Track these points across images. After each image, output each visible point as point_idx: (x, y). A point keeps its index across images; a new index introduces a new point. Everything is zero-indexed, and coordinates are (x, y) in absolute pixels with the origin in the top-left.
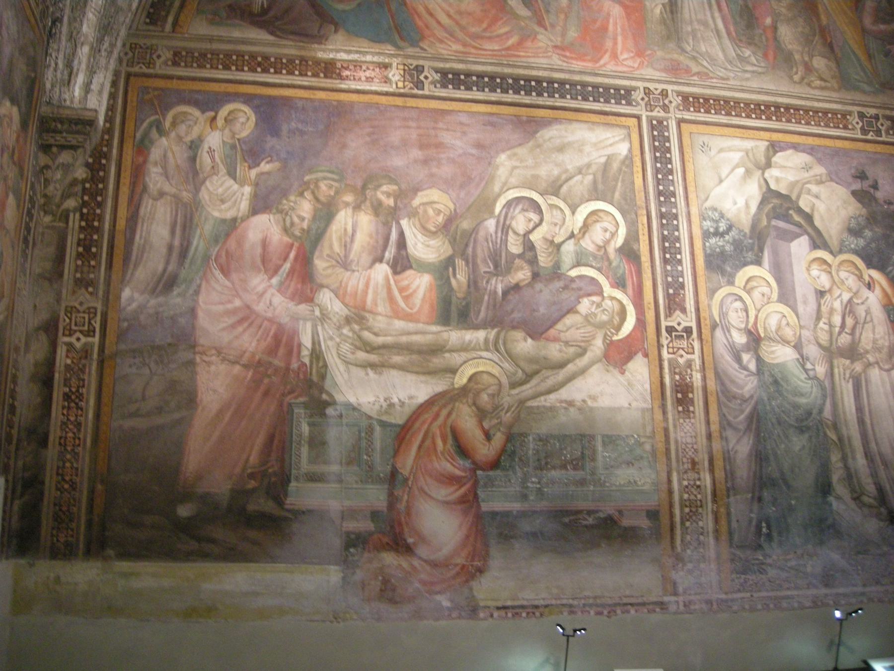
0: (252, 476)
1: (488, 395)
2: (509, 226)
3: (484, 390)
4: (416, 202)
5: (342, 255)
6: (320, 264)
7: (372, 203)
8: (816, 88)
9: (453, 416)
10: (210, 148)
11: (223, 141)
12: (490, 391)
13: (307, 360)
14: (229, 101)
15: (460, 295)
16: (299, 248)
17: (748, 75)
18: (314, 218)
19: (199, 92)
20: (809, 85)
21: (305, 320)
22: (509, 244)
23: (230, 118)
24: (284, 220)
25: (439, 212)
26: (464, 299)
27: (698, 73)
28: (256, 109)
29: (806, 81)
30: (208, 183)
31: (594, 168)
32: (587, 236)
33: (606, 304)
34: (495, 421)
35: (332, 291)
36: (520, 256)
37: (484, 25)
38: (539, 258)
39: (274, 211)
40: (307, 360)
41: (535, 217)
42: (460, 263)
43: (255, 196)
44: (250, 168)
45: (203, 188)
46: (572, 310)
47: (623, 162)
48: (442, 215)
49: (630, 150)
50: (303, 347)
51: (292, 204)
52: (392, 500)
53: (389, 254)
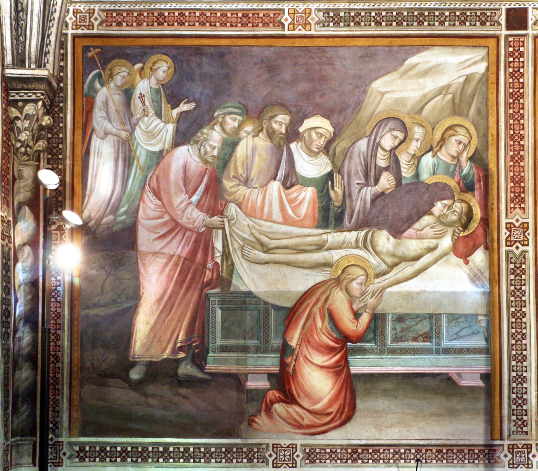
0: (181, 349)
1: (358, 284)
2: (379, 144)
3: (354, 279)
4: (301, 129)
5: (244, 176)
6: (227, 184)
7: (268, 133)
9: (329, 301)
10: (141, 94)
11: (151, 87)
12: (359, 280)
13: (219, 260)
14: (153, 54)
15: (337, 204)
16: (211, 173)
18: (222, 149)
19: (128, 47)
21: (217, 228)
22: (377, 158)
23: (155, 67)
24: (199, 150)
25: (321, 135)
26: (339, 207)
28: (174, 58)
30: (140, 123)
31: (452, 90)
32: (443, 148)
33: (456, 206)
34: (362, 304)
35: (237, 204)
36: (387, 169)
38: (402, 169)
39: (192, 142)
40: (219, 260)
41: (400, 135)
42: (337, 178)
43: (177, 132)
44: (172, 108)
45: (137, 128)
46: (428, 212)
47: (480, 81)
48: (324, 138)
49: (488, 69)
50: (216, 251)
51: (205, 136)
52: (283, 365)
53: (281, 173)
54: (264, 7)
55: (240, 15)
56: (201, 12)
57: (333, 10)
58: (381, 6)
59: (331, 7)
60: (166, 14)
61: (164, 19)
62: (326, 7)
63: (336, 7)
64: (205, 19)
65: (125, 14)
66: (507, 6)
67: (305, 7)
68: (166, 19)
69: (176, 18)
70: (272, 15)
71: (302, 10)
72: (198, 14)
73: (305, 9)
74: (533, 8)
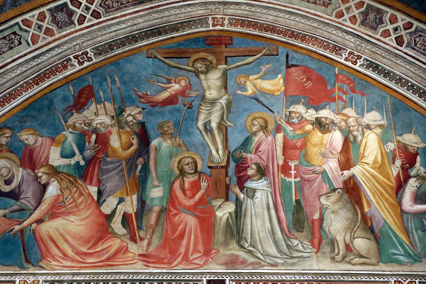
8: (354, 265)
17: (296, 260)
20: (349, 262)
27: (252, 263)
29: (347, 259)
37: (89, 245)
58: (100, 278)
59: (57, 279)
62: (52, 279)
63: (61, 279)
66: (207, 278)
67: (34, 279)
71: (31, 281)
73: (34, 280)
74: (230, 280)
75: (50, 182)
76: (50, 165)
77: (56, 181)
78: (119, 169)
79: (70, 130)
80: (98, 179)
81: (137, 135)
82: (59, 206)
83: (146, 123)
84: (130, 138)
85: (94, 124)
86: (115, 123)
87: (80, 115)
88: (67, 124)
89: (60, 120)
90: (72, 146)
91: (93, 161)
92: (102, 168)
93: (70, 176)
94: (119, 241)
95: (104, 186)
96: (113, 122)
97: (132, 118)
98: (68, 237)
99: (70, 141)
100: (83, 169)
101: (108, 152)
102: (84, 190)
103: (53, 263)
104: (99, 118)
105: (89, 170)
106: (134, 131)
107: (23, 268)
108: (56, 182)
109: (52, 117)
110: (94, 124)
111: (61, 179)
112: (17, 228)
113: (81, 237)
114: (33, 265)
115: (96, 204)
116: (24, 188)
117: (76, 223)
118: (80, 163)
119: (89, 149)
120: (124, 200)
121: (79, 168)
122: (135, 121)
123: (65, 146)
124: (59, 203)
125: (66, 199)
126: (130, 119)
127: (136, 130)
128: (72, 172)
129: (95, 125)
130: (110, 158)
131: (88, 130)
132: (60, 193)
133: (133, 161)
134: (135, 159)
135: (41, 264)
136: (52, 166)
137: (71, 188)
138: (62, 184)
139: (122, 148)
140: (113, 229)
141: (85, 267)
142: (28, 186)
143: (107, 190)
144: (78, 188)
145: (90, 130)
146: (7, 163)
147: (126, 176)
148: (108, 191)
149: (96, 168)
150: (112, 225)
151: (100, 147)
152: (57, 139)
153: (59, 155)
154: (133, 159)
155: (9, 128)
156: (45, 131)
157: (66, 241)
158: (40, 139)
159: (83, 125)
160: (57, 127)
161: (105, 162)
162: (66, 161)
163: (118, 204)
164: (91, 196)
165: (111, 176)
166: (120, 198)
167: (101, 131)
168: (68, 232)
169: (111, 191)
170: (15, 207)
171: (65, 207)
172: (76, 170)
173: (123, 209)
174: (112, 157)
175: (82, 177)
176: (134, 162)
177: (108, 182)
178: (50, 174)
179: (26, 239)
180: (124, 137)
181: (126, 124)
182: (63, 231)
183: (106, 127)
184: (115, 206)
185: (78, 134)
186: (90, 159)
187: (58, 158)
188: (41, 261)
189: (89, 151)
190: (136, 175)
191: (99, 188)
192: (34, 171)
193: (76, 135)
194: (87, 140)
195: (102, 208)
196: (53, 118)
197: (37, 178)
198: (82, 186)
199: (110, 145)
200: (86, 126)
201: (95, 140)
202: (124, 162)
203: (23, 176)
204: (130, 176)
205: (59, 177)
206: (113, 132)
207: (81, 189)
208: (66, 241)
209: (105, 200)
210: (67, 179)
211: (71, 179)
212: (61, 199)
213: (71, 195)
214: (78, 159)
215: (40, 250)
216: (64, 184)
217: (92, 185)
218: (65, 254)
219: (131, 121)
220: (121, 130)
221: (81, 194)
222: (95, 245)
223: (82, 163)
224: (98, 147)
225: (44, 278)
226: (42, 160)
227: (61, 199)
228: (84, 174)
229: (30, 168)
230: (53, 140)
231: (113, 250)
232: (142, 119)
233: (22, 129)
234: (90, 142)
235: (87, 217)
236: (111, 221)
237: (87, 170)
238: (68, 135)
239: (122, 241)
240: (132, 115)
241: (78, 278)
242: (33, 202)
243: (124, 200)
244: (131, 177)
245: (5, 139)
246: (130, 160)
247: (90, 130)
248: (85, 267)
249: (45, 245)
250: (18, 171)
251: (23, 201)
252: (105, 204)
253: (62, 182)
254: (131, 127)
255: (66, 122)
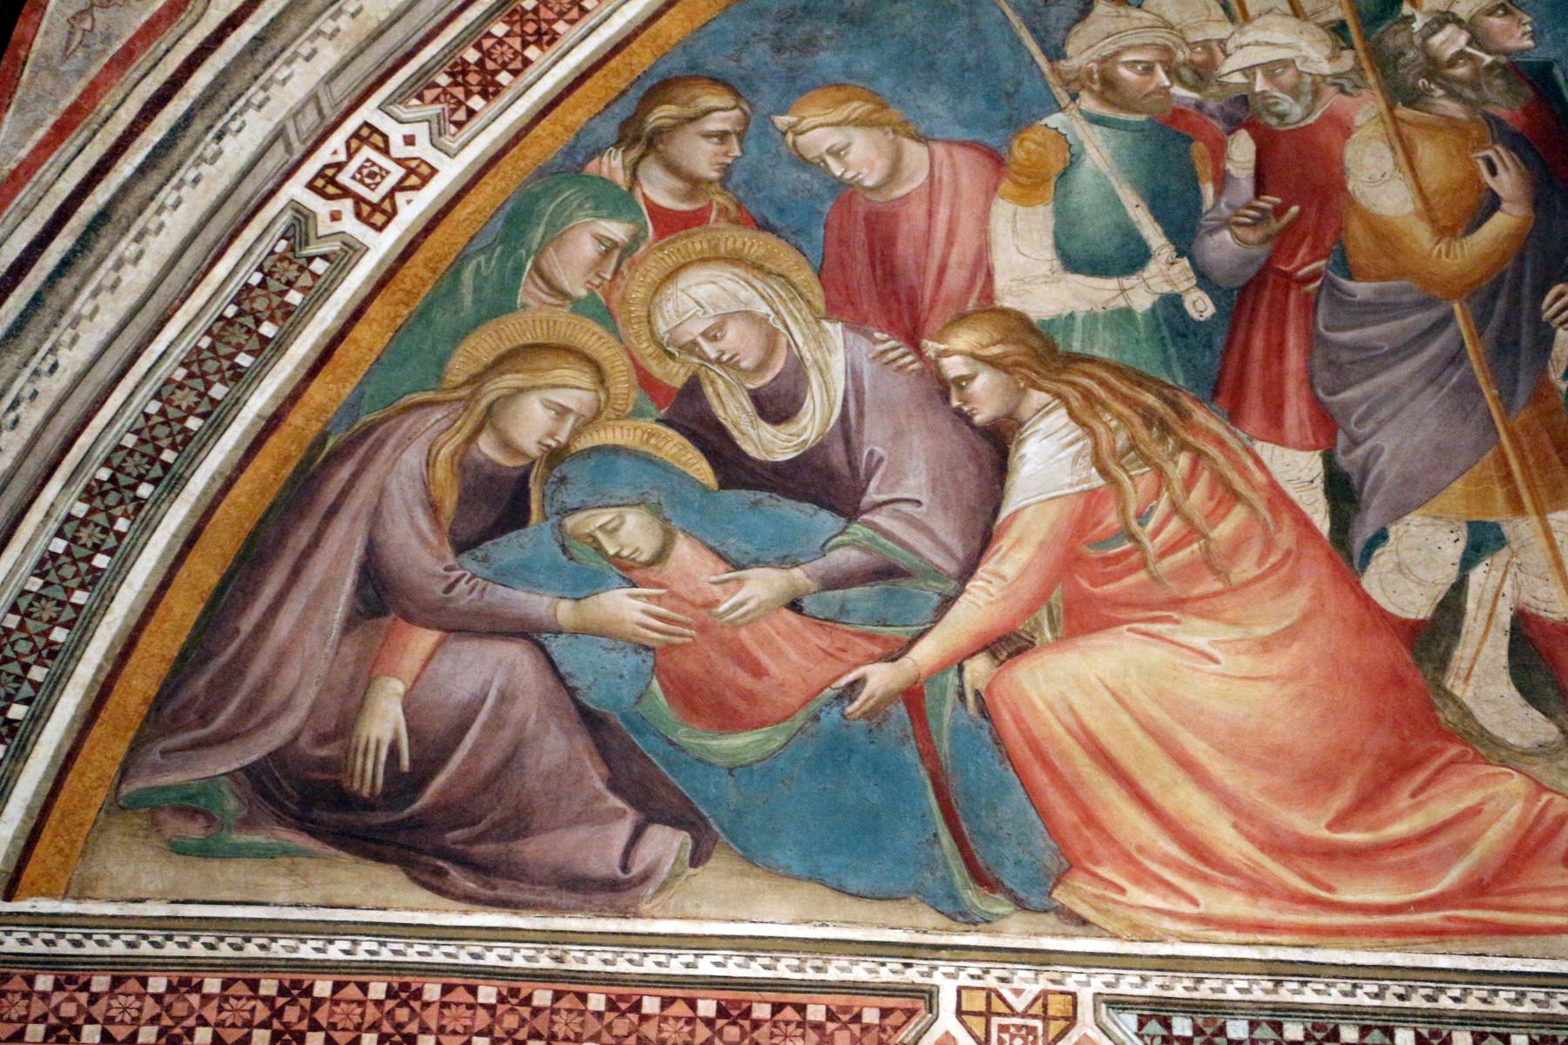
54: (833, 974)
55: (707, 1008)
56: (504, 986)
57: (1189, 1007)
58: (1445, 1002)
59: (1178, 991)
60: (323, 988)
61: (309, 1014)
62: (1151, 989)
64: (523, 1021)
65: (100, 983)
67: (1043, 984)
68: (322, 1016)
69: (372, 1013)
70: (871, 1016)
72: (487, 994)
73: (1044, 995)
75: (1026, 411)
76: (1005, 312)
77: (1063, 411)
78: (1433, 349)
79: (1088, 103)
80: (1315, 402)
81: (1515, 142)
82: (1106, 561)
83: (1557, 71)
84: (1472, 162)
85: (1231, 69)
86: (1358, 69)
87: (1136, 13)
88: (1063, 65)
89: (1017, 43)
90: (1117, 203)
91: (1267, 294)
92: (1326, 342)
93: (1141, 380)
94: (1516, 784)
95: (1361, 451)
96: (1347, 60)
97: (1463, 38)
98: (1199, 749)
99: (1098, 174)
100: (1209, 345)
101: (1351, 249)
102: (1243, 471)
103: (1137, 895)
104: (1251, 34)
105: (1247, 346)
106: (1494, 122)
107: (969, 919)
108: (1060, 417)
109: (964, 22)
110: (1231, 69)
111: (1087, 395)
112: (880, 678)
113: (1278, 751)
114: (1021, 905)
115: (1330, 556)
116: (874, 438)
117: (1228, 663)
118: (1188, 305)
119: (1227, 224)
120: (1501, 541)
121: (1184, 336)
122: (1488, 59)
123: (1075, 201)
124: (1101, 542)
125: (1142, 517)
126: (1449, 41)
127: (1502, 113)
128: (1145, 358)
129: (1238, 78)
130: (1366, 278)
131: (1199, 106)
132: (1098, 482)
133: (1515, 301)
134: (1526, 291)
135: (1060, 896)
136: (1022, 319)
137: (1159, 452)
138: (1100, 429)
139: (1433, 221)
140: (1467, 714)
141: (1340, 932)
142: (898, 436)
143: (1380, 478)
144: (1198, 455)
145: (1211, 105)
146: (745, 293)
147: (1489, 393)
148: (1390, 476)
149: (1293, 340)
150: (1453, 683)
151: (1295, 209)
152: (1019, 154)
153: (1049, 254)
154: (1516, 288)
155: (717, 81)
156: (936, 106)
157: (1188, 766)
158: (915, 154)
159: (1161, 77)
160: (1009, 87)
161: (1341, 303)
162: (1096, 293)
163: (1468, 562)
164: (1291, 505)
165: (1395, 390)
166: (1471, 525)
167: (1281, 116)
168: (1194, 719)
169: (1407, 480)
170: (845, 557)
171: (1144, 564)
172: (1172, 351)
173: (1507, 589)
174: (1381, 278)
175: (1216, 393)
176: (1526, 304)
177: (1381, 424)
178: (1017, 364)
179: (944, 747)
180: (1429, 153)
181: (1430, 77)
182: (1155, 711)
183: (1307, 88)
184: (1450, 574)
185: (1138, 129)
186: (1241, 282)
187: (1045, 269)
188: (1058, 881)
189: (1226, 235)
190: (1551, 387)
191: (1329, 460)
192: (917, 348)
193: (1128, 138)
194: (1204, 169)
195: (1371, 582)
196: (975, 30)
197: (942, 388)
198: (1220, 443)
199: (1352, 201)
200: (1184, 84)
201: (1251, 165)
202: (1456, 306)
203: (854, 374)
204: (1513, 393)
205: (1073, 384)
206: (1359, 120)
207: (1221, 459)
208: (1188, 766)
209: (1381, 537)
210: (1125, 399)
211: (1151, 399)
212: (1112, 520)
213: (1165, 495)
214: (1169, 281)
215: (1044, 814)
216: (1115, 430)
217: (1281, 441)
218: (1199, 850)
219: (1461, 54)
220: (1402, 112)
221: (1227, 495)
222: (1368, 802)
223: (1200, 306)
224: (1279, 211)
225: (1099, 981)
226: (956, 278)
227: (1112, 520)
228: (1221, 374)
229: (891, 327)
230: (997, 160)
231: (1493, 838)
232: (1529, 43)
233: (795, 87)
234: (1222, 180)
235: (1291, 634)
236: (1443, 663)
237: (1237, 348)
238: (1081, 136)
239: (1541, 788)
240: (1459, 22)
241: (1309, 997)
242: (946, 528)
243: (1501, 541)
244: (1521, 398)
245: (709, 147)
246: (1494, 295)
247: (1211, 105)
248: (1340, 932)
249: (1070, 791)
250: (819, 340)
251: (881, 519)
252: (1383, 559)
253: (1097, 416)
254: (1468, 93)
255: (1056, 53)
